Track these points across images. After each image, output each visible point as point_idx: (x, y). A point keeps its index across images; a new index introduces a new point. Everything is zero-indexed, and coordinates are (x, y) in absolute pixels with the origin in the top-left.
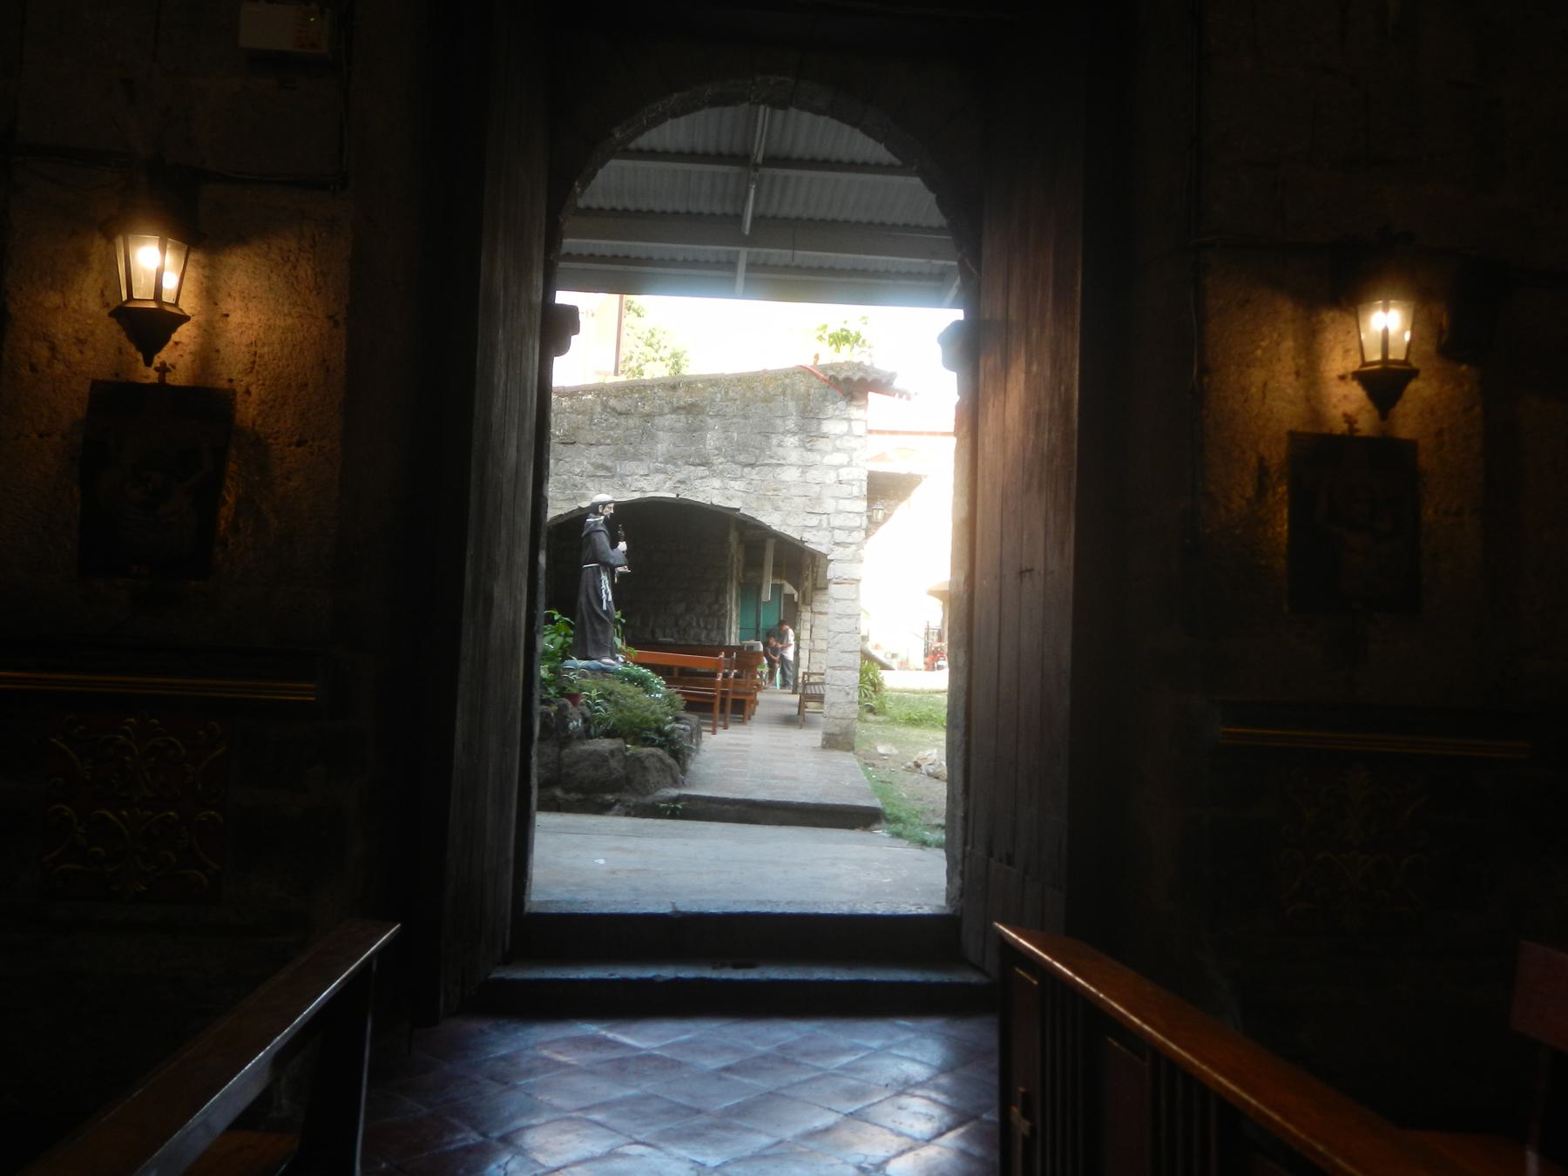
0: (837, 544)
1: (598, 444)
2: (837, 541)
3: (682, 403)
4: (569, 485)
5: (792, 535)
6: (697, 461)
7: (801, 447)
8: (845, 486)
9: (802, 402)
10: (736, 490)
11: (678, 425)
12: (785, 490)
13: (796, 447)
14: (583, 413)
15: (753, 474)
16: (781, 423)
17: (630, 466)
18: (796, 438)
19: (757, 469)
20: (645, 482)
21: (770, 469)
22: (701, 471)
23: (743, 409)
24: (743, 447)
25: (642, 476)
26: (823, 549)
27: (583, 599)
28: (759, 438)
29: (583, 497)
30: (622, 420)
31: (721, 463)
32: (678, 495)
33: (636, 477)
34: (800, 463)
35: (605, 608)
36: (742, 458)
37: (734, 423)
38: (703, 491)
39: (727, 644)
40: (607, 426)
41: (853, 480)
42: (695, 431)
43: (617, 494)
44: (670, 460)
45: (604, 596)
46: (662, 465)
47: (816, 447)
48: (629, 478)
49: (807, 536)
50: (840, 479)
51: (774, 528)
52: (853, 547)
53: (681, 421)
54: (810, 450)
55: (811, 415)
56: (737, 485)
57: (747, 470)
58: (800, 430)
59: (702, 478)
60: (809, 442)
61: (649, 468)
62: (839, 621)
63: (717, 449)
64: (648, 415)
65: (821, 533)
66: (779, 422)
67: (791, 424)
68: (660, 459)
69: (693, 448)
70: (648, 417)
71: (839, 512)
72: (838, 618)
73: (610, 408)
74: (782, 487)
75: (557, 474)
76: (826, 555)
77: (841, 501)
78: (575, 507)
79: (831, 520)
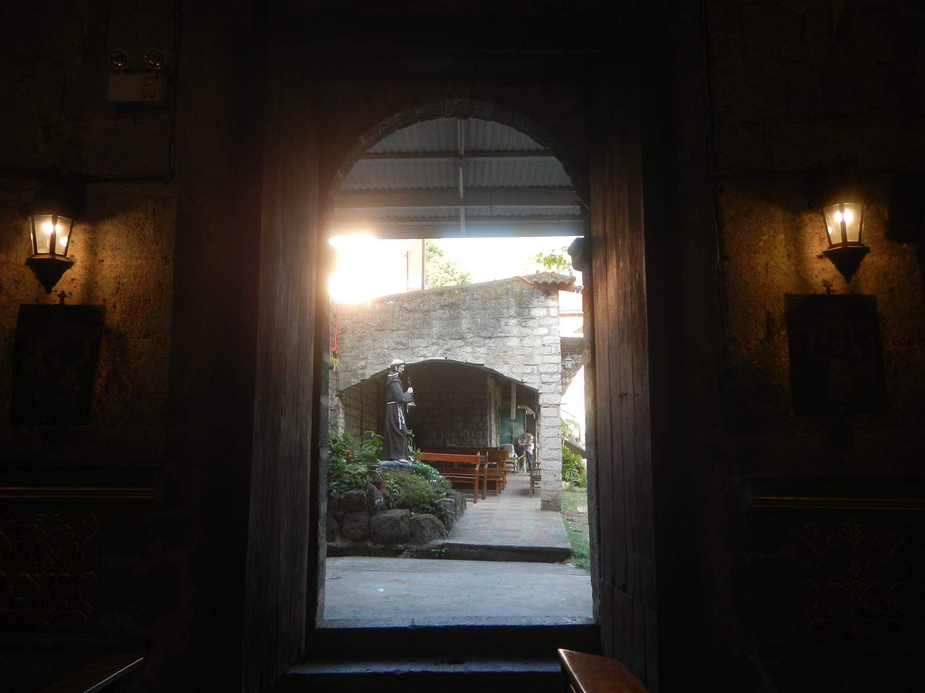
0: (544, 383)
1: (398, 330)
3: (446, 303)
4: (381, 355)
7: (519, 325)
15: (491, 343)
16: (506, 312)
17: (417, 342)
18: (516, 320)
20: (426, 351)
21: (501, 339)
22: (459, 343)
23: (483, 304)
24: (484, 327)
25: (424, 347)
26: (535, 387)
27: (387, 424)
28: (493, 321)
31: (471, 338)
32: (446, 358)
33: (421, 348)
35: (400, 428)
36: (483, 334)
37: (478, 313)
38: (461, 355)
39: (489, 446)
40: (402, 319)
41: (551, 344)
42: (455, 319)
43: (410, 359)
44: (441, 337)
45: (400, 421)
47: (528, 325)
48: (417, 349)
49: (525, 379)
51: (505, 375)
52: (554, 385)
53: (446, 313)
54: (524, 327)
55: (524, 306)
56: (482, 350)
57: (487, 341)
58: (518, 315)
59: (460, 347)
60: (524, 322)
61: (428, 343)
63: (468, 329)
64: (427, 311)
65: (534, 377)
66: (505, 311)
67: (512, 312)
68: (435, 337)
69: (454, 329)
71: (544, 364)
72: (546, 429)
73: (404, 308)
75: (374, 349)
76: (538, 390)
77: (545, 357)
78: (386, 368)
79: (540, 368)
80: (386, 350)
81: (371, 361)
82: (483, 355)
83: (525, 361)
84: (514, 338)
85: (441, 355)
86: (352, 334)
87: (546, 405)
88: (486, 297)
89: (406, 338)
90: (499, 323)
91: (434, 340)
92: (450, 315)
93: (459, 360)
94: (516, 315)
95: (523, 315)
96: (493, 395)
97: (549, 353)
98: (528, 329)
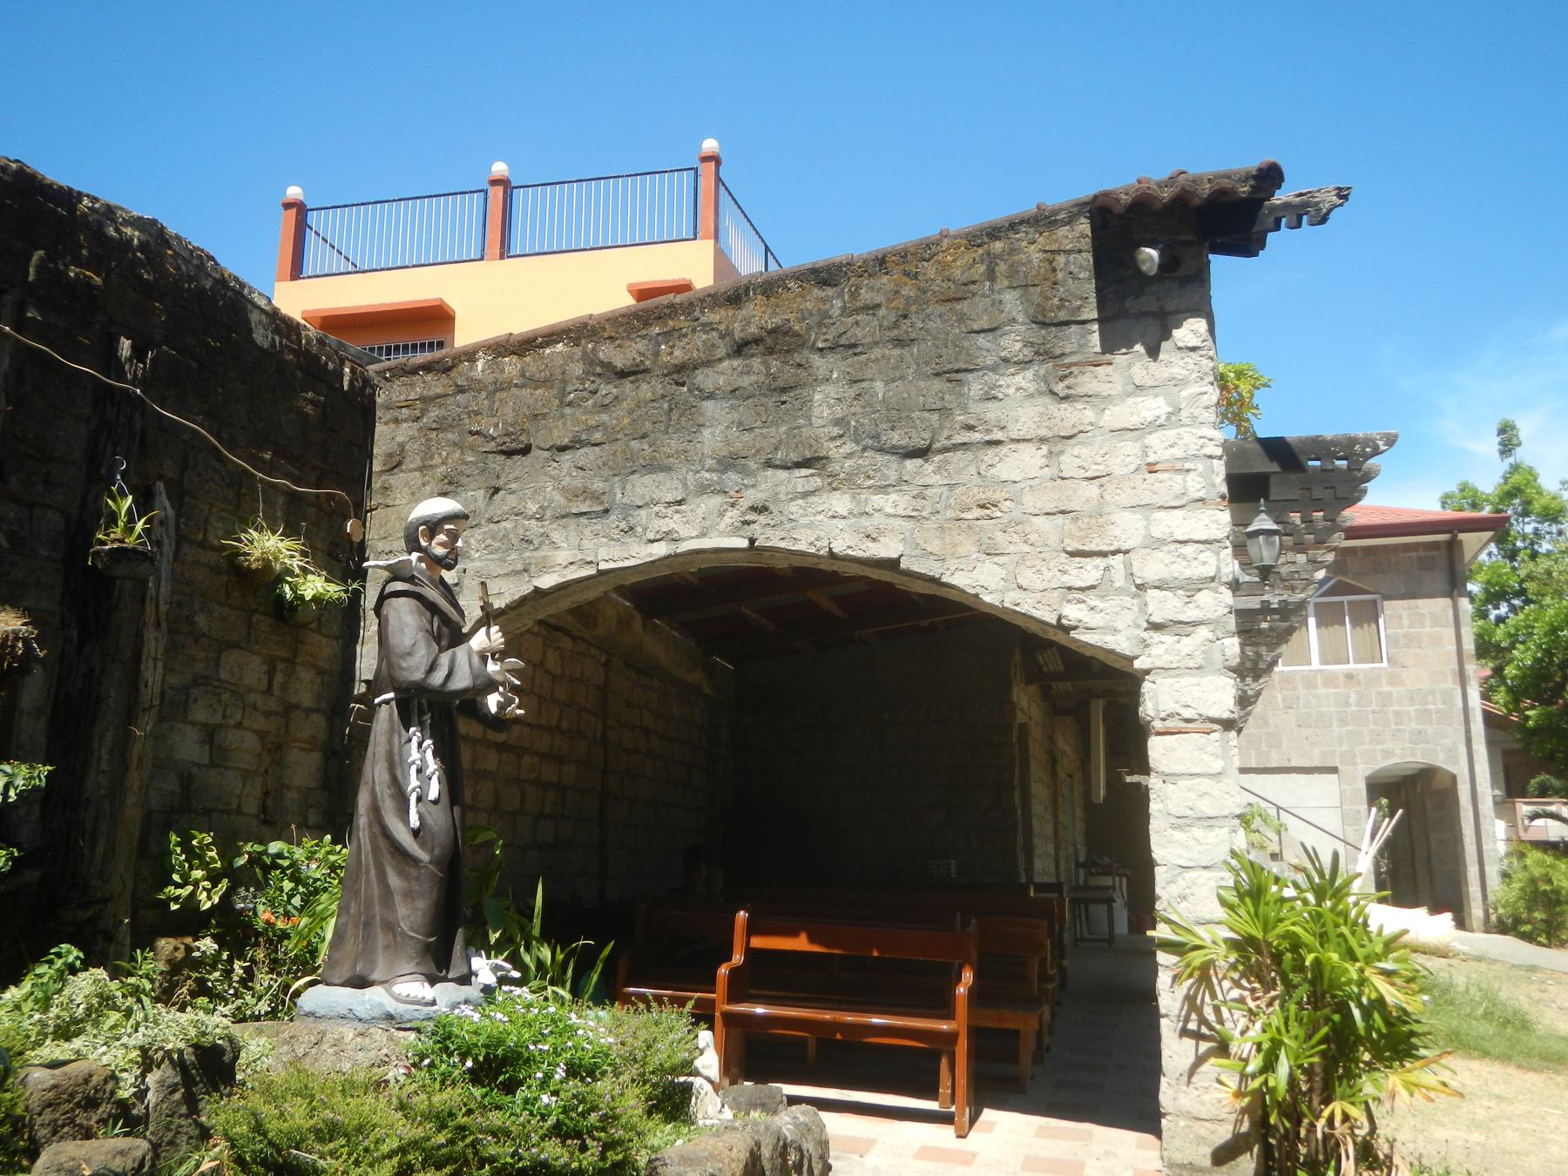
0: (1156, 627)
2: (1156, 619)
3: (753, 329)
4: (515, 541)
5: (1037, 614)
6: (794, 457)
7: (1041, 393)
8: (1166, 475)
9: (1038, 289)
10: (888, 515)
11: (745, 381)
12: (1008, 503)
13: (1031, 396)
14: (545, 383)
17: (643, 486)
18: (1029, 374)
19: (937, 458)
20: (676, 517)
21: (969, 455)
22: (801, 479)
23: (896, 325)
24: (897, 414)
26: (1119, 640)
27: (363, 800)
28: (938, 384)
29: (545, 567)
30: (627, 386)
31: (849, 456)
32: (752, 541)
33: (656, 509)
34: (1043, 432)
35: (414, 821)
36: (896, 438)
37: (877, 360)
40: (594, 406)
42: (784, 390)
44: (730, 462)
45: (414, 782)
46: (715, 477)
47: (1080, 390)
48: (643, 513)
49: (1073, 613)
50: (1151, 459)
51: (987, 598)
52: (1203, 633)
54: (1066, 398)
55: (1063, 316)
57: (911, 464)
58: (1037, 353)
59: (805, 495)
60: (1062, 379)
61: (685, 486)
62: (1178, 835)
63: (837, 422)
64: (681, 368)
65: (1111, 604)
66: (981, 340)
67: (1012, 344)
68: (709, 462)
69: (783, 429)
70: (680, 372)
71: (1155, 544)
72: (1174, 827)
73: (602, 364)
74: (998, 496)
75: (490, 520)
76: (1131, 659)
78: (526, 589)
79: (1136, 564)
80: (533, 522)
81: (478, 564)
82: (896, 523)
83: (1071, 536)
84: (1021, 446)
85: (735, 531)
86: (420, 469)
87: (1170, 724)
88: (908, 298)
89: (606, 472)
90: (961, 395)
91: (707, 475)
92: (768, 375)
93: (802, 546)
94: (1028, 353)
95: (1058, 352)
96: (1036, 733)
97: (1177, 497)
98: (1079, 406)
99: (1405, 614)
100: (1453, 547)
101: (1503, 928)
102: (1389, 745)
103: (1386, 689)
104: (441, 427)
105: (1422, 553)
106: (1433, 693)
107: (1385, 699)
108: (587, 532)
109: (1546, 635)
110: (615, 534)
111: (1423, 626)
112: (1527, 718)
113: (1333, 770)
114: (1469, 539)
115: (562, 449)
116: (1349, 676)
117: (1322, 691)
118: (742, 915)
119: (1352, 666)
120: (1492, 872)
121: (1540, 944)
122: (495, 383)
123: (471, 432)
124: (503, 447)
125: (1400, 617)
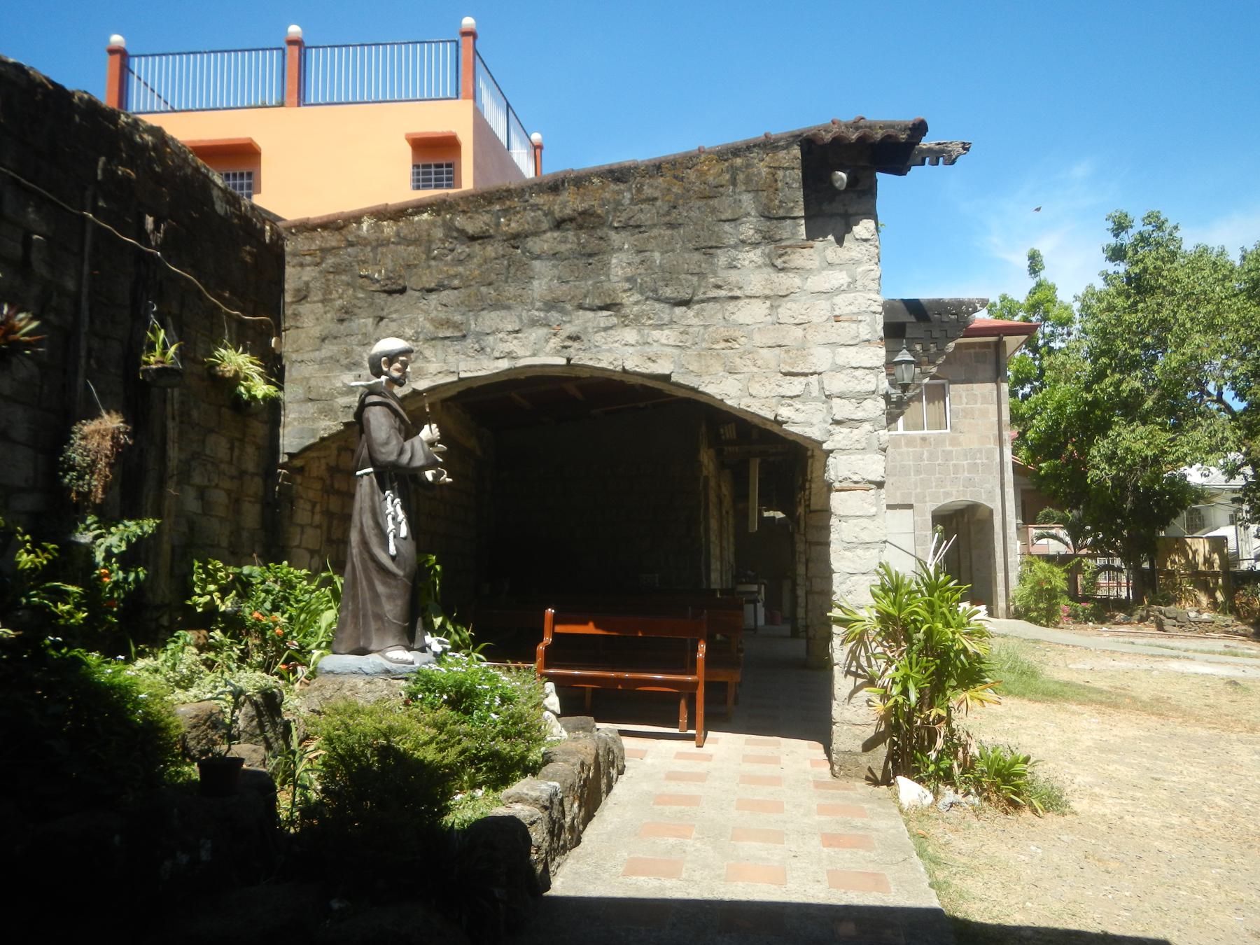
0: (837, 422)
1: (440, 288)
2: (838, 417)
3: (568, 211)
5: (762, 413)
6: (598, 302)
7: (766, 265)
8: (846, 324)
9: (765, 194)
10: (663, 345)
11: (563, 248)
12: (743, 339)
13: (760, 267)
14: (416, 242)
15: (688, 315)
16: (731, 230)
17: (490, 319)
18: (758, 251)
19: (696, 307)
20: (515, 342)
21: (718, 306)
23: (668, 213)
24: (669, 275)
25: (510, 333)
26: (815, 433)
27: (354, 537)
28: (697, 256)
30: (477, 247)
31: (637, 303)
32: (569, 360)
33: (501, 335)
34: (767, 292)
35: (392, 550)
36: (668, 292)
37: (655, 237)
38: (610, 350)
39: (704, 587)
40: (453, 260)
41: (859, 313)
42: (590, 255)
43: (472, 364)
44: (552, 305)
45: (391, 526)
46: (542, 314)
47: (792, 265)
48: (491, 338)
49: (785, 413)
50: (837, 313)
51: (729, 402)
53: (570, 240)
54: (782, 270)
55: (781, 213)
56: (666, 336)
57: (679, 311)
58: (764, 238)
59: (606, 329)
60: (781, 256)
61: (521, 320)
62: (847, 554)
63: (628, 280)
65: (810, 407)
66: (727, 227)
67: (748, 230)
68: (538, 304)
69: (590, 282)
70: (516, 239)
71: (839, 369)
72: (845, 549)
73: (457, 230)
74: (737, 334)
76: (821, 443)
77: (842, 349)
79: (826, 382)
82: (669, 350)
83: (785, 362)
84: (753, 301)
85: (557, 352)
86: (322, 301)
87: (845, 485)
88: (676, 195)
89: (463, 309)
90: (712, 264)
91: (536, 313)
92: (579, 244)
93: (604, 365)
94: (758, 237)
95: (778, 237)
96: (712, 483)
97: (853, 338)
98: (791, 275)
99: (964, 394)
100: (999, 346)
101: (1018, 615)
102: (948, 489)
103: (949, 448)
104: (337, 270)
105: (977, 350)
106: (980, 451)
107: (947, 456)
108: (450, 350)
109: (1054, 410)
110: (471, 352)
111: (976, 403)
112: (1041, 469)
113: (910, 506)
114: (1011, 341)
115: (430, 291)
116: (924, 439)
117: (904, 449)
118: (550, 611)
119: (926, 431)
120: (1013, 576)
121: (1041, 625)
122: (377, 240)
123: (361, 277)
124: (386, 288)
125: (961, 397)
